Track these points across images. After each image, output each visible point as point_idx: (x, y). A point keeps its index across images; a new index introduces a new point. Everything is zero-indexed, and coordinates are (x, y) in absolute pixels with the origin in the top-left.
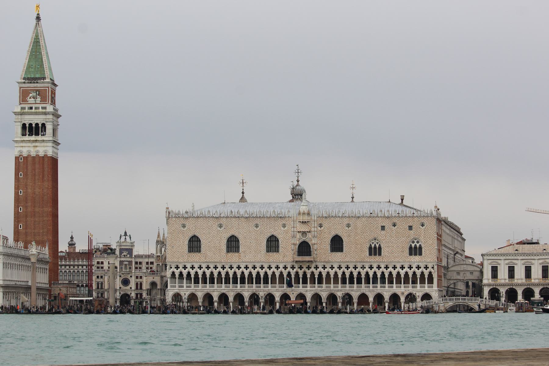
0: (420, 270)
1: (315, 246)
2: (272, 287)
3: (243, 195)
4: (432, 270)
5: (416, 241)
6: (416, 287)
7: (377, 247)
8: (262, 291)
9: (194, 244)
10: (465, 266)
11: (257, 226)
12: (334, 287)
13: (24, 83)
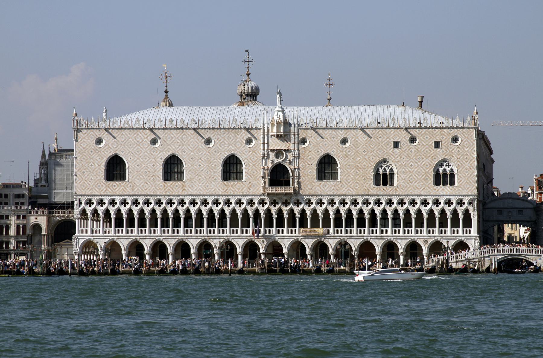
1: (296, 173)
3: (167, 95)
4: (471, 209)
6: (446, 232)
7: (388, 173)
8: (216, 238)
9: (115, 168)
10: (510, 201)
11: (208, 142)
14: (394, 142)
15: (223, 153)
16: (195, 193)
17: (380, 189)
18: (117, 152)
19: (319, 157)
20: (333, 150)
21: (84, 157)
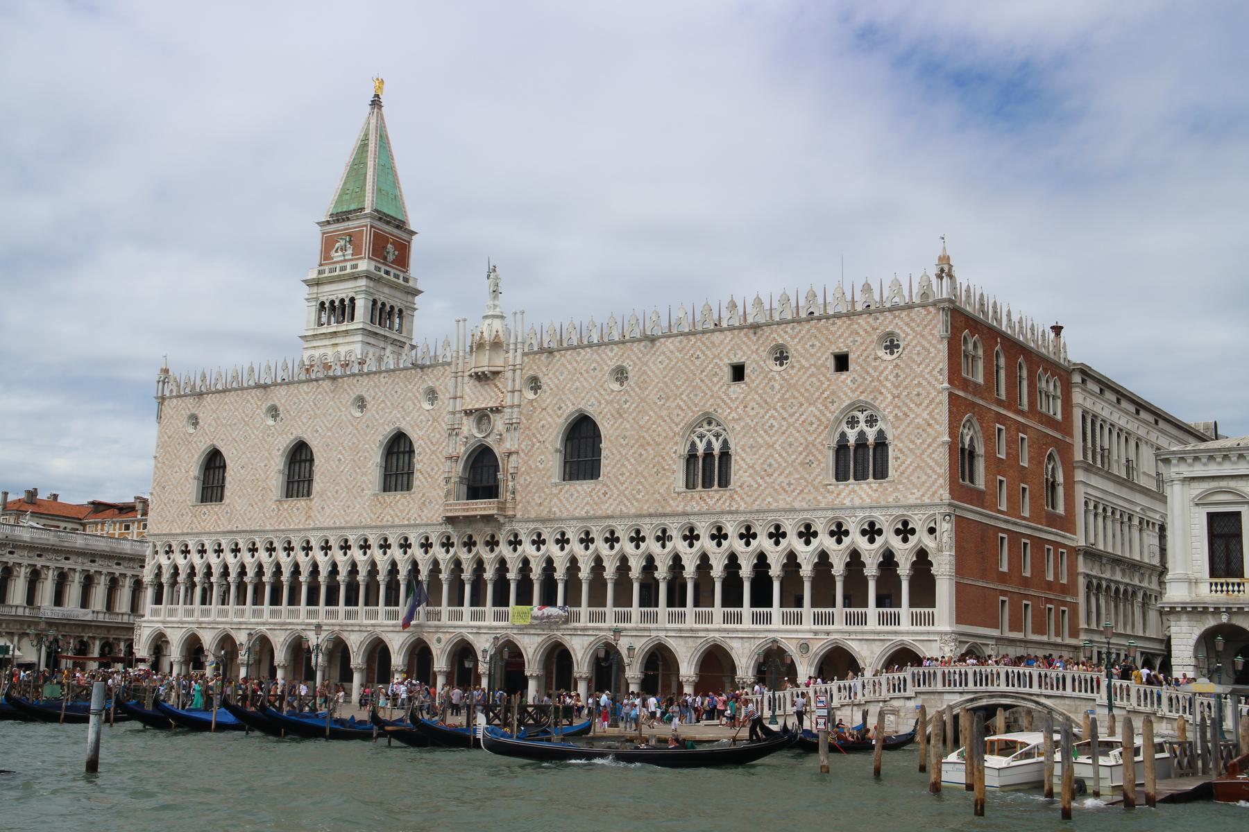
0: (879, 540)
4: (929, 543)
5: (862, 417)
6: (863, 620)
7: (716, 452)
11: (361, 403)
13: (328, 222)
15: (380, 429)
16: (326, 525)
19: (561, 421)
20: (593, 400)
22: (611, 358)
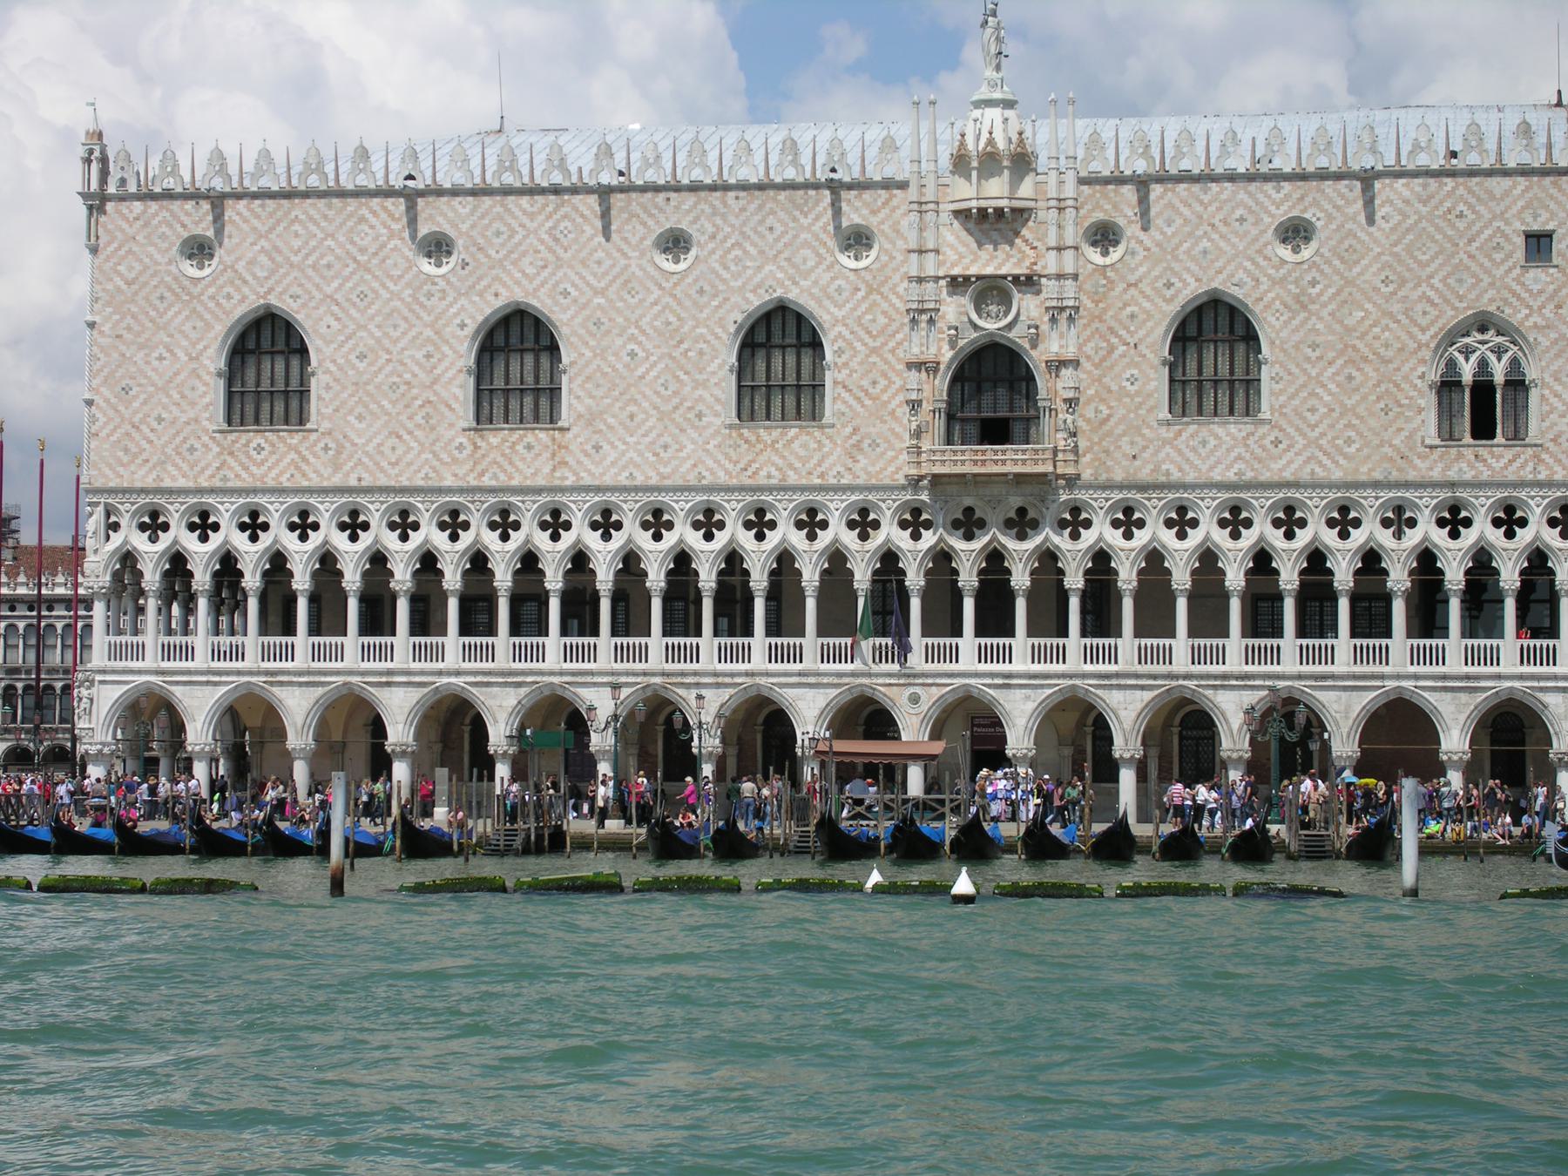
2: (775, 654)
8: (710, 678)
12: (1197, 656)
14: (1529, 236)
16: (608, 480)
17: (1460, 456)
18: (273, 300)
20: (1241, 275)
21: (129, 320)
22: (1281, 203)
